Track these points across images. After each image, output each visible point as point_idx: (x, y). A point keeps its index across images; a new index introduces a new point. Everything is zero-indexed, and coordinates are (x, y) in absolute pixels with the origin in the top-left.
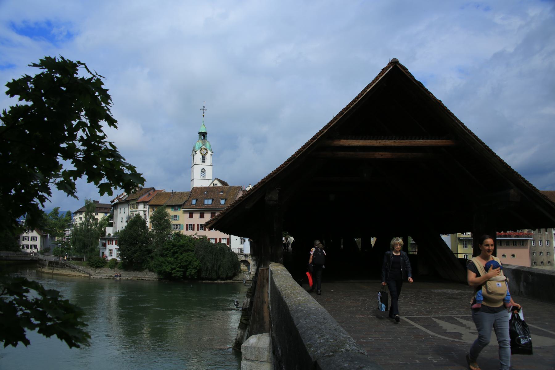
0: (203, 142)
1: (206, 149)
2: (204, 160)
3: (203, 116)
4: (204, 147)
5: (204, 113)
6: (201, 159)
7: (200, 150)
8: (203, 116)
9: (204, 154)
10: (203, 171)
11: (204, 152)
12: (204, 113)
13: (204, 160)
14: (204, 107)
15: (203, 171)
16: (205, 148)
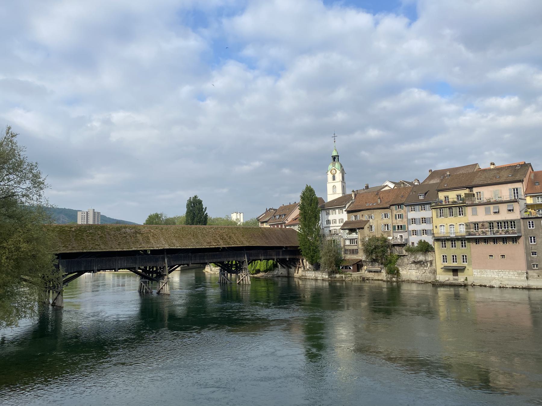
0: (333, 164)
1: (335, 169)
2: (334, 179)
3: (335, 142)
4: (333, 168)
5: (335, 139)
6: (332, 178)
7: (331, 171)
8: (335, 142)
9: (334, 174)
10: (334, 187)
11: (334, 171)
12: (335, 139)
13: (334, 179)
14: (334, 134)
15: (335, 187)
16: (334, 169)
